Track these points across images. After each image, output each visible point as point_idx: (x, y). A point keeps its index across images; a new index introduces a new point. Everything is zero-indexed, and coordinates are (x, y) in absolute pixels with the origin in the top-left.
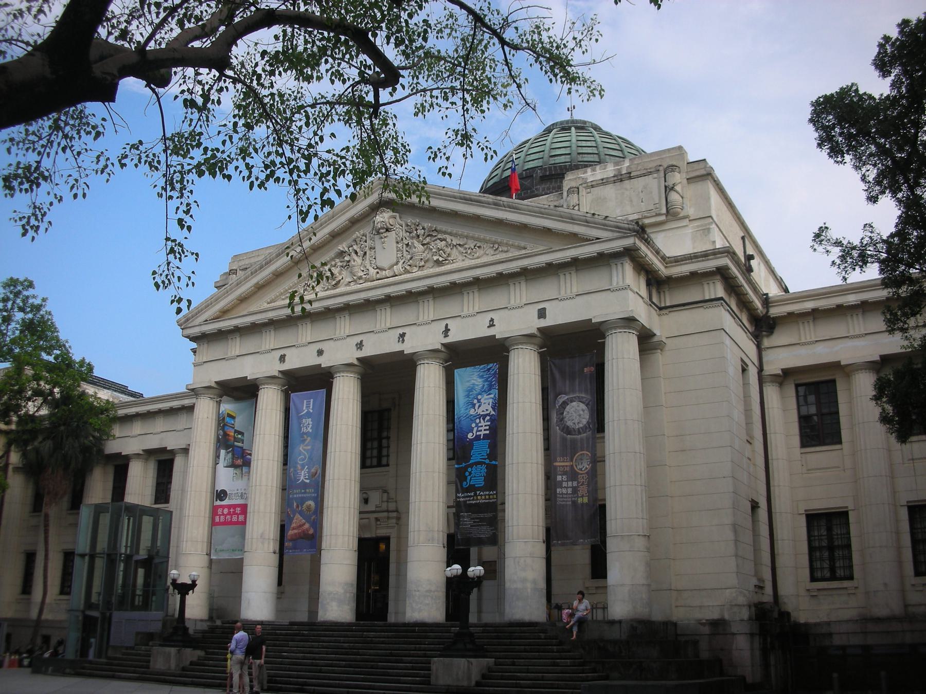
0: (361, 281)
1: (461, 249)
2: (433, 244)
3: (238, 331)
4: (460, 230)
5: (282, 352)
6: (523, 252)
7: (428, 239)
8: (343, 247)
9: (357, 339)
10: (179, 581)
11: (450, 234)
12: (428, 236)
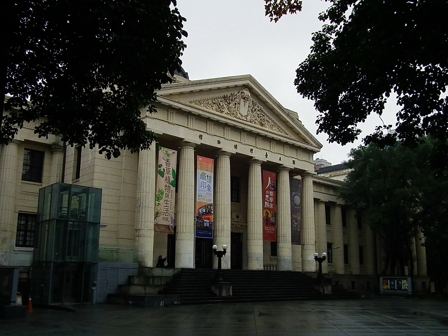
3: (180, 112)
4: (270, 116)
5: (201, 134)
9: (236, 143)
10: (217, 251)
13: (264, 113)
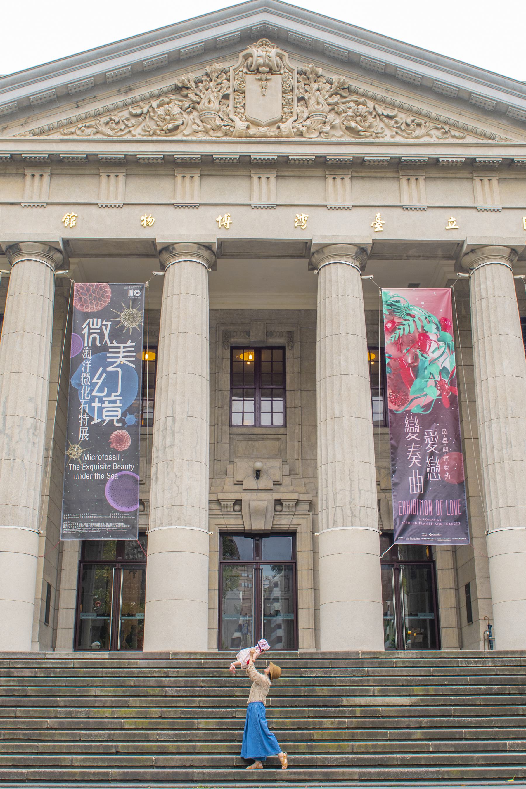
0: (219, 134)
1: (392, 122)
2: (342, 107)
6: (490, 142)
7: (336, 99)
8: (188, 77)
11: (373, 98)
12: (336, 94)
13: (364, 95)
